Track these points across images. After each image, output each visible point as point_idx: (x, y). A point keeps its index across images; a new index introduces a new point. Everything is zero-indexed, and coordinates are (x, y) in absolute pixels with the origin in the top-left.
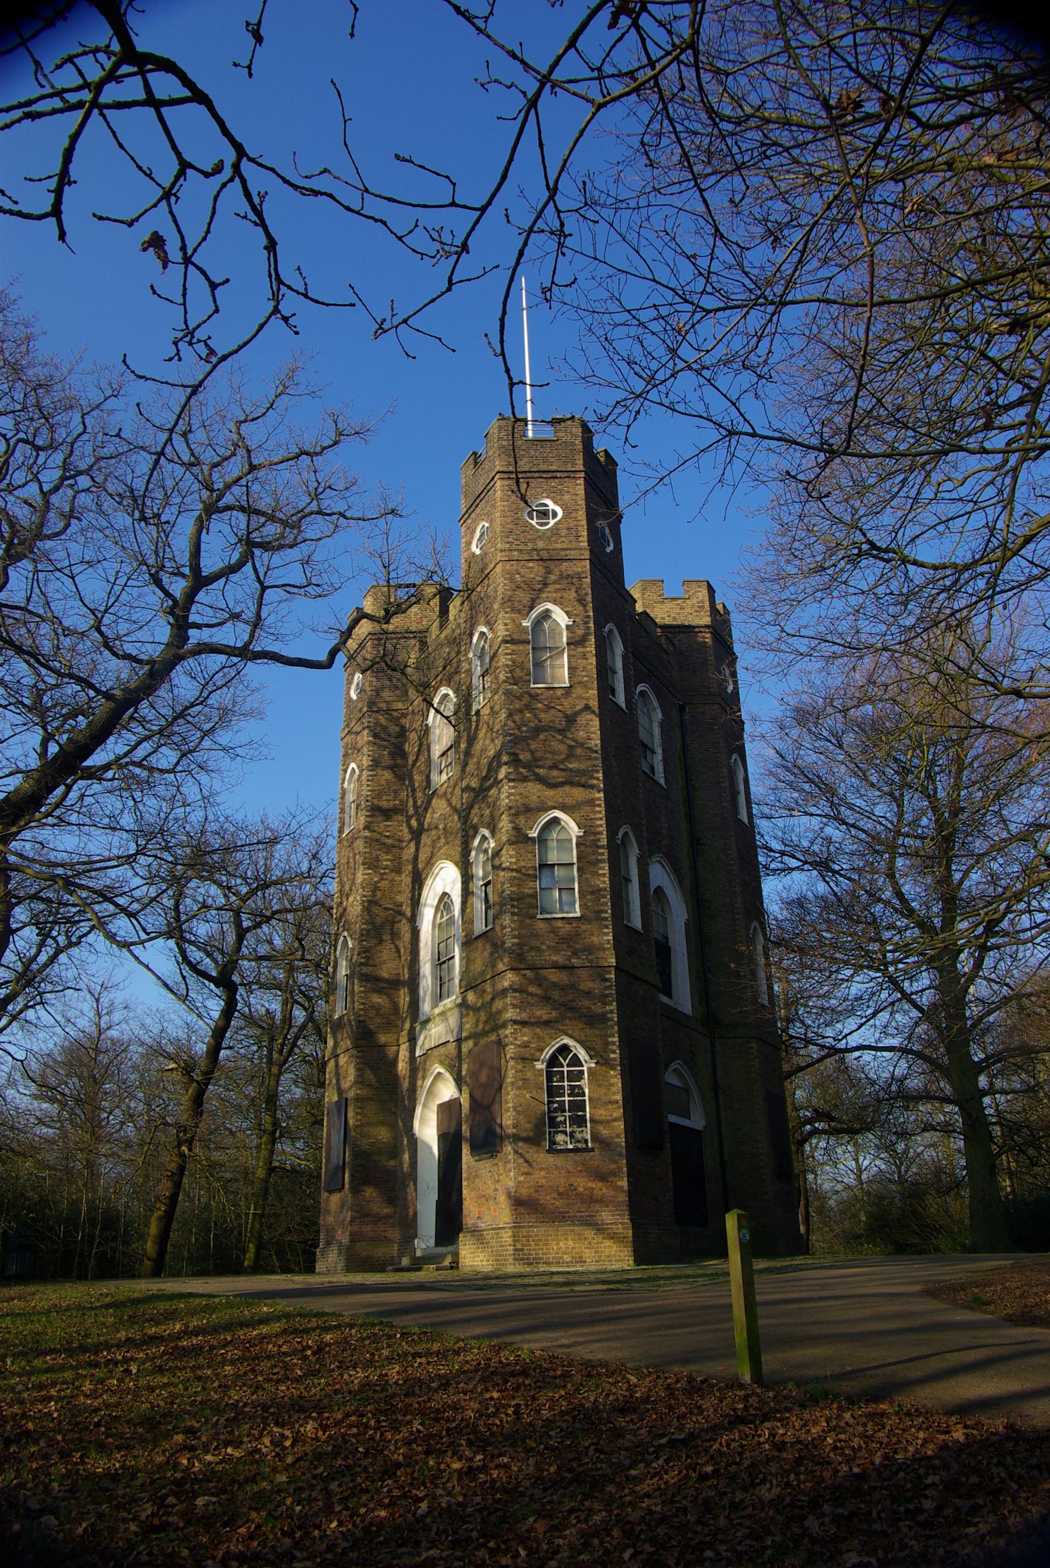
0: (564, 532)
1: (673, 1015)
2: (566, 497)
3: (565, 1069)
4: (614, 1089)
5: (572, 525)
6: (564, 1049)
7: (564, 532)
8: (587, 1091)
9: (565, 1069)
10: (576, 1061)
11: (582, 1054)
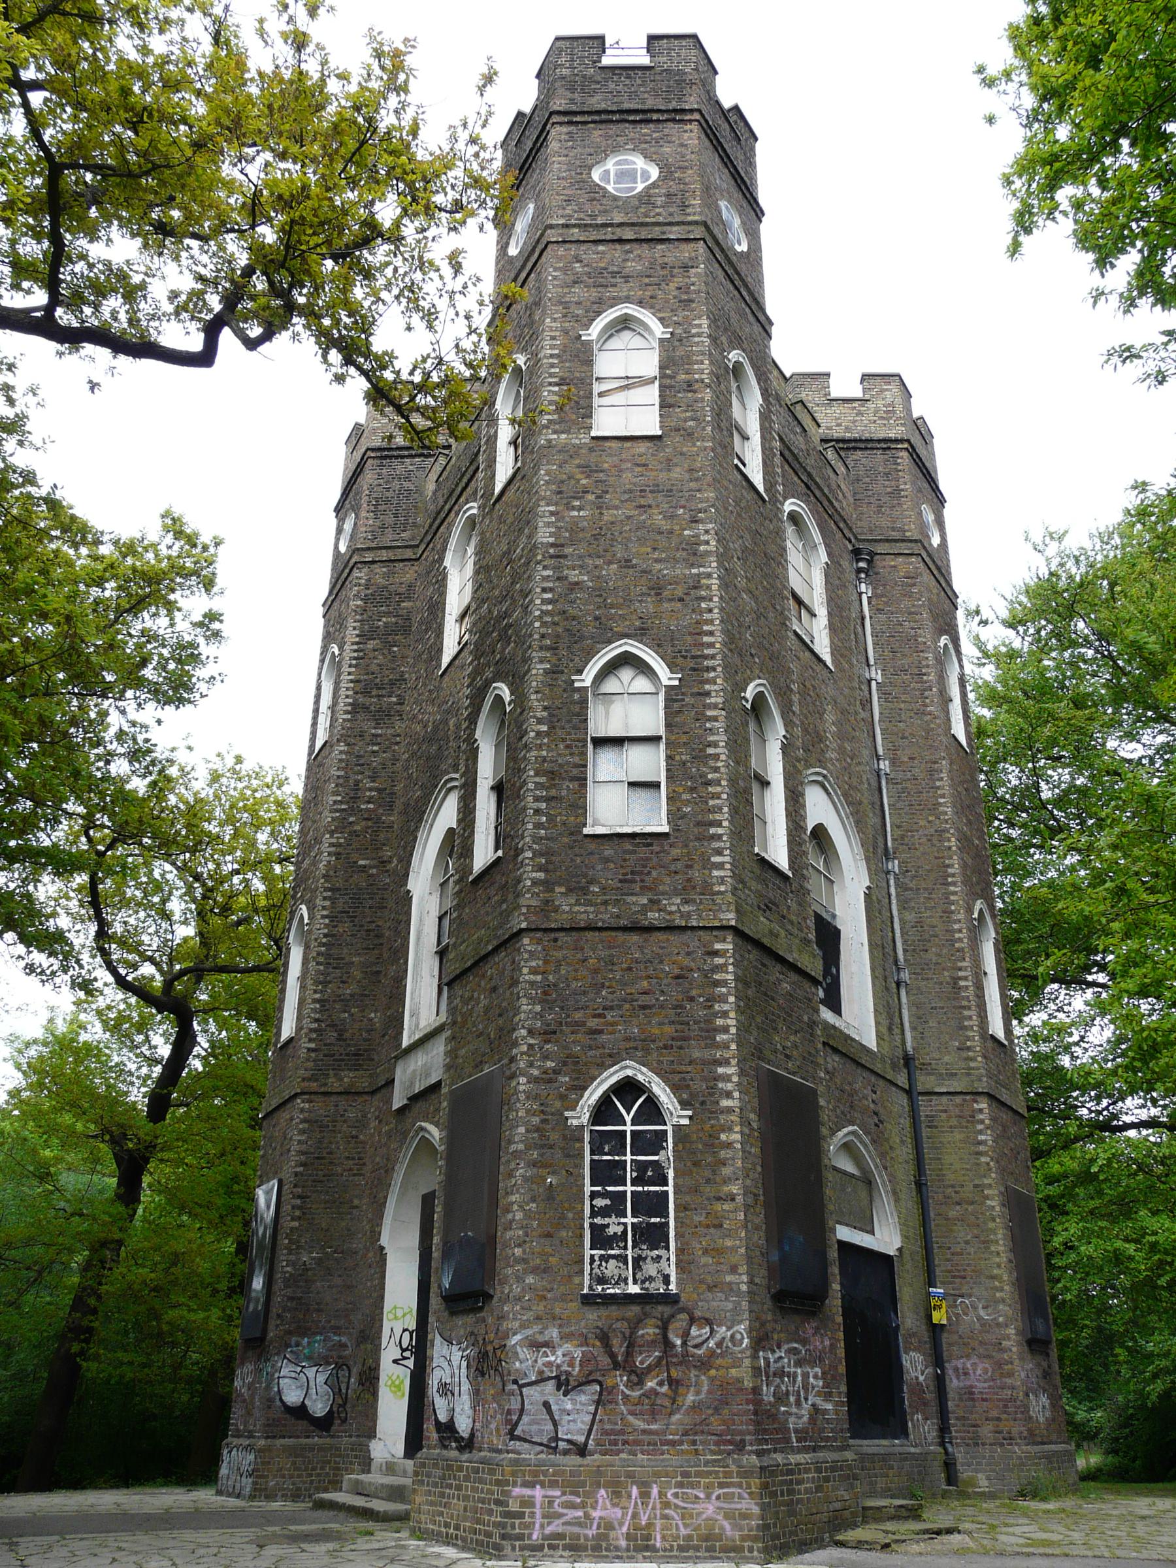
0: (660, 201)
1: (842, 1047)
3: (629, 1128)
4: (726, 1171)
5: (674, 190)
6: (628, 1089)
8: (671, 1174)
9: (629, 1128)
10: (652, 1111)
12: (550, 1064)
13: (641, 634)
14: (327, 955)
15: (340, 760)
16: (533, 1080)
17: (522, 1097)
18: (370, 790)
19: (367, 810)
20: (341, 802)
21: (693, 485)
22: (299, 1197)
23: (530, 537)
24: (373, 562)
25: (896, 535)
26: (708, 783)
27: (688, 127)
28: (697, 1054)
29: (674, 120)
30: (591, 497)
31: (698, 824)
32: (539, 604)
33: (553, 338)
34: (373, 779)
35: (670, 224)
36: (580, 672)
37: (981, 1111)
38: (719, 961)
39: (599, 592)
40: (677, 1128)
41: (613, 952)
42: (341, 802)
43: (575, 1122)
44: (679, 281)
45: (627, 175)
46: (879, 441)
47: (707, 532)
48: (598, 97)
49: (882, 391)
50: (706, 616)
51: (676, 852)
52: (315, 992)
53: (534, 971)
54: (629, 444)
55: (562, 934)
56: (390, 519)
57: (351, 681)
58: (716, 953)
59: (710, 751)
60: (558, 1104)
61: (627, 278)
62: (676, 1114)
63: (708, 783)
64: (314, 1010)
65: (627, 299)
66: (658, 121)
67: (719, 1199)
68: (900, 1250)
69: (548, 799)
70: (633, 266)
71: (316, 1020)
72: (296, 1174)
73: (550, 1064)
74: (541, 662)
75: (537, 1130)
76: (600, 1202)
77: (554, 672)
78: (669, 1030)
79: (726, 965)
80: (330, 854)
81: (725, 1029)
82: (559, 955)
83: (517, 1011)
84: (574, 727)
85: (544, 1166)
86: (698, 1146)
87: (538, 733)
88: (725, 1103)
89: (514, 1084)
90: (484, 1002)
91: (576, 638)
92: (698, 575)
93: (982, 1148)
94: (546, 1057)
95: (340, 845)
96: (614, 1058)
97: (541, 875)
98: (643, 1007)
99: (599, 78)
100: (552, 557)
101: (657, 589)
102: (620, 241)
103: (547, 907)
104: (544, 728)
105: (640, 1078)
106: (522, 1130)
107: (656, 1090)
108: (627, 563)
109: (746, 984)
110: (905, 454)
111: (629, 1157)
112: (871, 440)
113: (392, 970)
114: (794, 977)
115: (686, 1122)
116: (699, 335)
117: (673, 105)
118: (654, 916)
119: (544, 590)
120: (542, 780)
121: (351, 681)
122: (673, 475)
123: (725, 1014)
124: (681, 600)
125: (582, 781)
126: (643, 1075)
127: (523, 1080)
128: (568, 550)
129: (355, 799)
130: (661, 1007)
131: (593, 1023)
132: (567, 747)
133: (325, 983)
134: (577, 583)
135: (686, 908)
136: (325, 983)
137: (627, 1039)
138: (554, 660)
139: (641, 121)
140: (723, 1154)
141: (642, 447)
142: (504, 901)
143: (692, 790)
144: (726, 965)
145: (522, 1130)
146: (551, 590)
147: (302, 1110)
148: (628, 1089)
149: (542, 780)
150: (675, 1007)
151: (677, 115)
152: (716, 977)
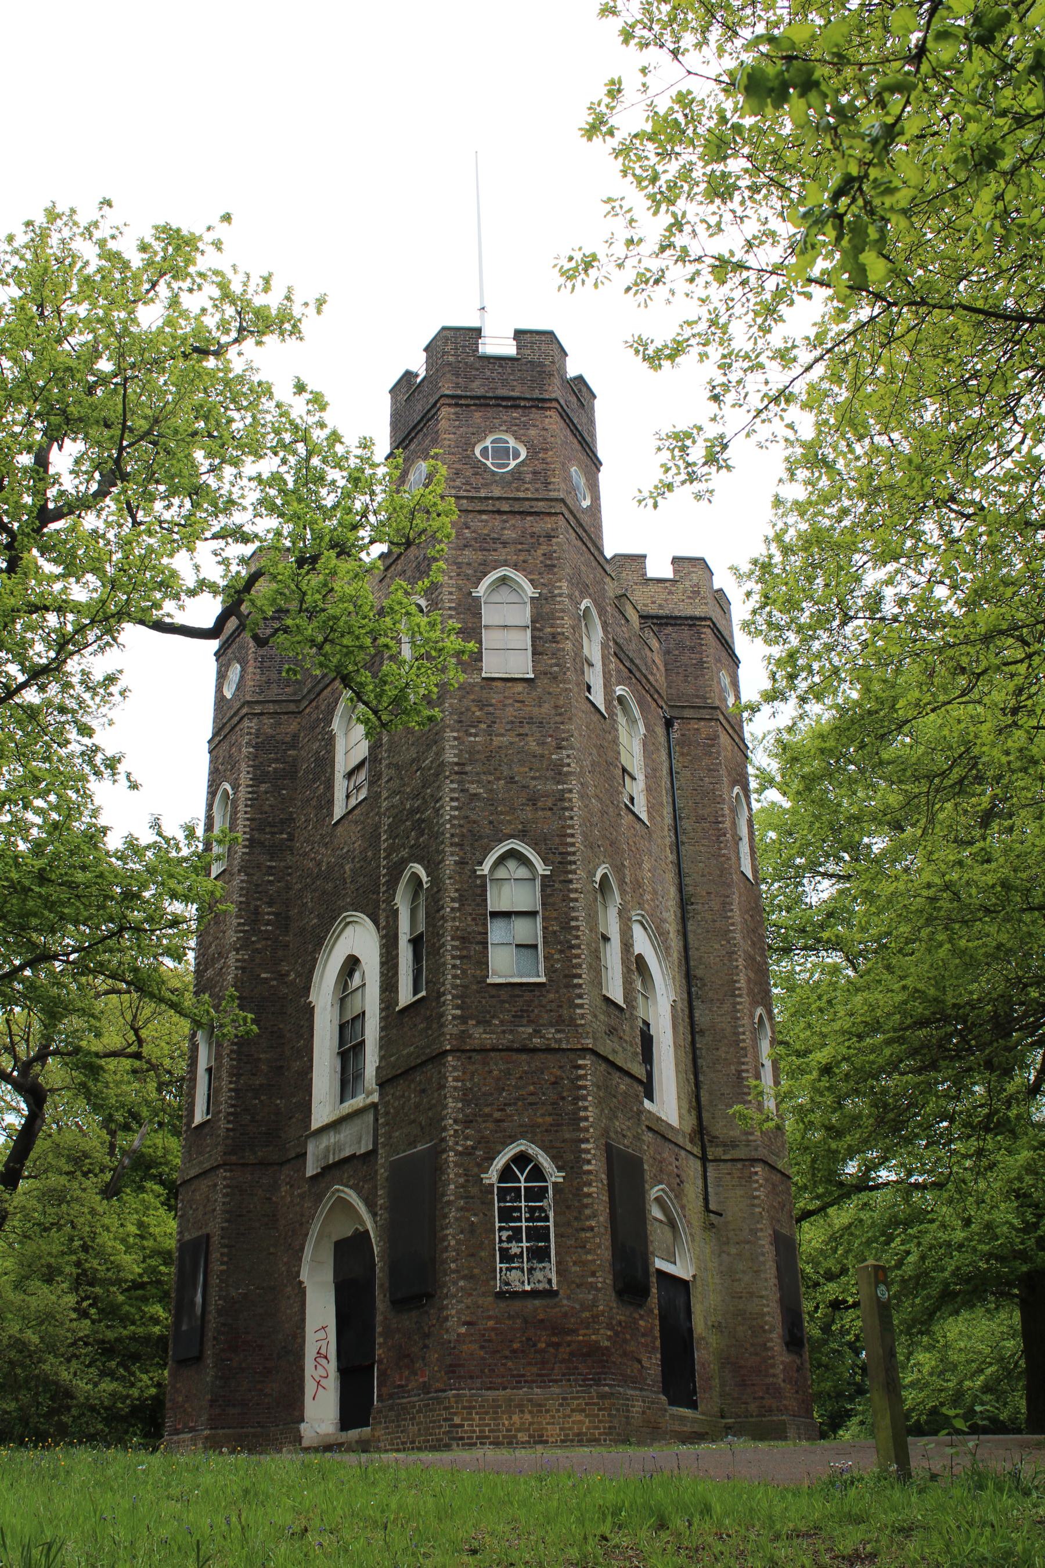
0: (528, 477)
2: (532, 432)
3: (523, 1185)
7: (528, 477)
8: (551, 1214)
9: (523, 1185)
10: (538, 1173)
11: (545, 1162)
12: (469, 1143)
13: (522, 835)
14: (238, 1052)
15: (242, 888)
16: (458, 1154)
17: (451, 1165)
18: (269, 914)
19: (266, 931)
20: (243, 924)
21: (558, 719)
22: (226, 1246)
23: (438, 754)
24: (262, 714)
25: (699, 702)
26: (572, 947)
27: (548, 413)
28: (567, 1136)
29: (537, 407)
30: (483, 726)
31: (566, 976)
32: (449, 810)
33: (451, 593)
34: (270, 904)
35: (537, 500)
36: (481, 863)
37: (756, 1173)
38: (581, 1072)
39: (491, 802)
40: (555, 1184)
41: (510, 1066)
42: (243, 924)
43: (488, 1181)
44: (544, 549)
45: (502, 453)
46: (686, 618)
47: (568, 756)
48: (477, 383)
49: (689, 573)
50: (569, 822)
51: (551, 996)
52: (231, 1082)
53: (456, 1079)
54: (509, 684)
55: (474, 1054)
56: (274, 676)
57: (248, 819)
58: (580, 1067)
59: (573, 923)
60: (476, 1170)
61: (505, 544)
62: (554, 1176)
63: (572, 947)
64: (230, 1098)
65: (505, 563)
66: (525, 407)
67: (583, 1229)
68: (694, 1276)
69: (461, 958)
70: (509, 534)
71: (232, 1106)
72: (223, 1229)
73: (469, 1143)
74: (452, 855)
75: (463, 1186)
76: (505, 1234)
77: (461, 863)
78: (549, 1119)
79: (586, 1075)
80: (237, 968)
81: (586, 1119)
82: (471, 1068)
83: (445, 1107)
84: (478, 905)
85: (468, 1210)
86: (570, 1198)
87: (453, 909)
88: (586, 1167)
89: (444, 1156)
90: (414, 1099)
91: (476, 837)
92: (563, 790)
93: (756, 1202)
94: (466, 1138)
95: (245, 961)
96: (513, 1139)
97: (458, 1012)
98: (531, 1104)
99: (477, 365)
100: (456, 773)
101: (533, 801)
102: (499, 512)
103: (463, 1035)
104: (456, 905)
105: (530, 1151)
106: (452, 1187)
107: (541, 1159)
108: (511, 780)
109: (598, 1087)
110: (708, 631)
111: (523, 1204)
112: (680, 618)
113: (296, 1065)
114: (627, 1080)
115: (561, 1180)
116: (560, 595)
117: (536, 394)
118: (536, 1041)
119: (452, 799)
120: (457, 943)
121: (248, 819)
122: (543, 710)
123: (586, 1109)
124: (551, 809)
125: (485, 944)
126: (533, 1150)
127: (451, 1154)
128: (468, 768)
129: (255, 922)
130: (543, 1104)
131: (497, 1115)
132: (474, 919)
133: (238, 1075)
134: (475, 795)
135: (558, 1036)
136: (238, 1075)
137: (521, 1126)
138: (461, 854)
139: (511, 407)
140: (586, 1201)
141: (519, 687)
142: (430, 1028)
143: (561, 952)
144: (586, 1075)
145: (452, 1187)
146: (457, 799)
147: (225, 1178)
148: (522, 1159)
149: (457, 943)
150: (553, 1104)
151: (540, 404)
152: (580, 1083)
